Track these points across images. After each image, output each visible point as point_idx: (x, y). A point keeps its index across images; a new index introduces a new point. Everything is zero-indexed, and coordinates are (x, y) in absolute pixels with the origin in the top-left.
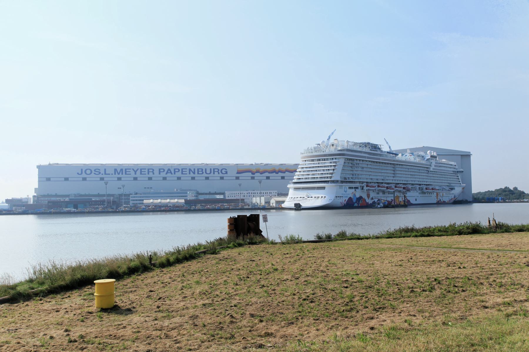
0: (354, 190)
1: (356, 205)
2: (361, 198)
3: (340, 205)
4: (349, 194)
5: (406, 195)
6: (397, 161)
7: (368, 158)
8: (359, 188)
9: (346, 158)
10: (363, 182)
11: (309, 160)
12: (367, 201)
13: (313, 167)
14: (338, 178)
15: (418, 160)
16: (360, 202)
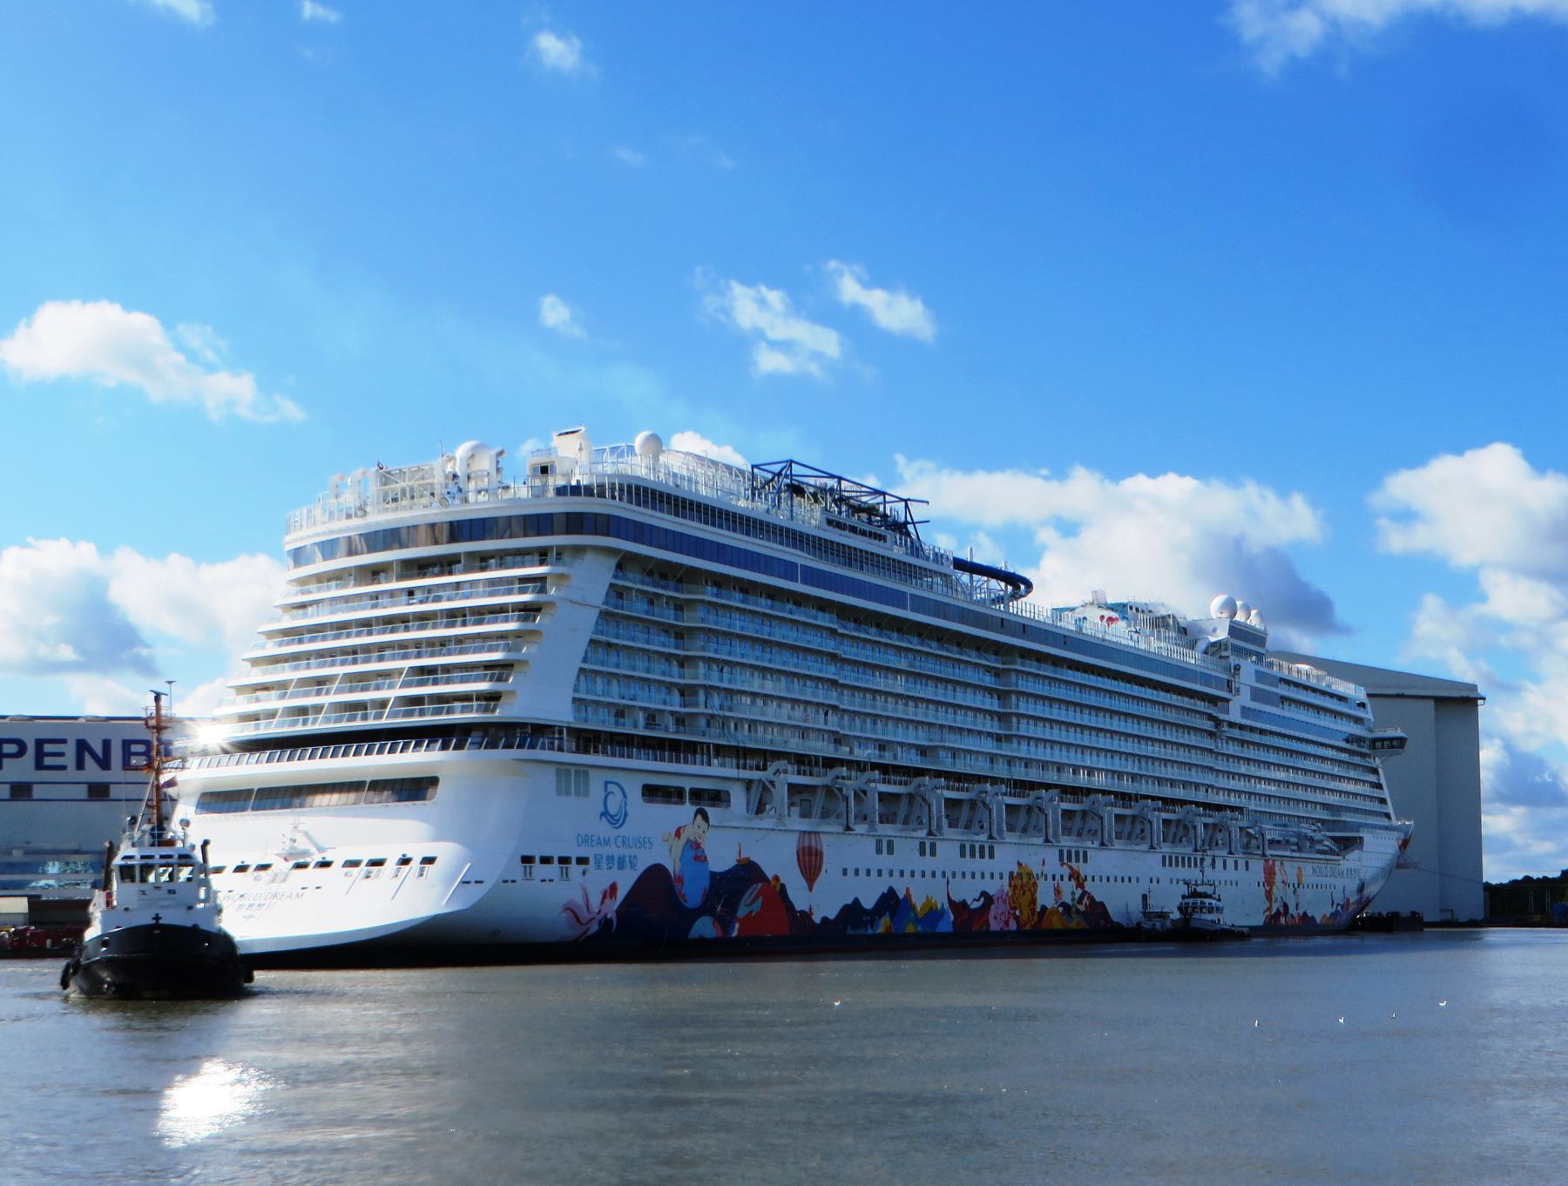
0: (688, 809)
1: (704, 927)
2: (747, 872)
3: (564, 929)
4: (644, 842)
5: (1084, 869)
6: (1026, 628)
7: (810, 576)
8: (738, 795)
9: (625, 562)
10: (766, 757)
11: (338, 576)
12: (800, 898)
13: (366, 624)
14: (557, 709)
15: (1154, 645)
16: (742, 911)
